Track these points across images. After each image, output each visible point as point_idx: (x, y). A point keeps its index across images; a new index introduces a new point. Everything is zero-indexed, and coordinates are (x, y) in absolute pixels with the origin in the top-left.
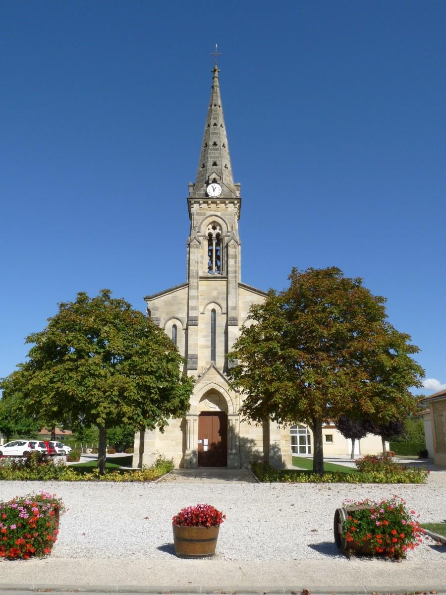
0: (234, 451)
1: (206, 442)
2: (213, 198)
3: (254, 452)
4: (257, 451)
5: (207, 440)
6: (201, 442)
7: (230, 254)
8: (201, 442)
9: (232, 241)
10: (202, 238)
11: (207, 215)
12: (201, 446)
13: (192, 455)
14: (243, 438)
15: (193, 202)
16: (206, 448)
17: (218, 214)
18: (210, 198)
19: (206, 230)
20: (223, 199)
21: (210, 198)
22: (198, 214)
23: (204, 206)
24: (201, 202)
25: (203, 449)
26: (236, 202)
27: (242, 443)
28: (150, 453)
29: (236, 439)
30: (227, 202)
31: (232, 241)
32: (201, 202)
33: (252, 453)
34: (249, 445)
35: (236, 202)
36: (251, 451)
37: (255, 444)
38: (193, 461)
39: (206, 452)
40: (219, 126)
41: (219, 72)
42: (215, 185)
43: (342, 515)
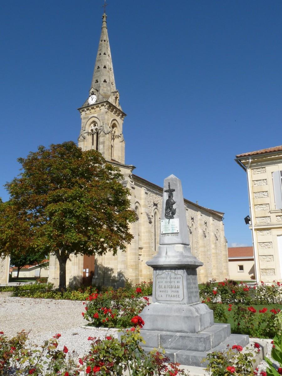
0: (96, 277)
1: (87, 270)
2: (91, 105)
3: (113, 277)
4: (114, 276)
5: (88, 269)
6: (84, 270)
7: (101, 141)
8: (84, 270)
9: (102, 132)
10: (86, 134)
11: (89, 118)
12: (85, 273)
13: (73, 279)
14: (106, 267)
15: (81, 111)
16: (87, 275)
17: (96, 115)
18: (90, 106)
19: (89, 128)
20: (97, 105)
21: (90, 106)
22: (85, 118)
23: (88, 112)
24: (85, 110)
25: (85, 276)
26: (105, 104)
27: (106, 271)
28: (52, 278)
29: (98, 269)
30: (100, 106)
31: (102, 132)
32: (85, 110)
33: (112, 278)
34: (110, 273)
35: (105, 104)
36: (111, 277)
37: (113, 272)
38: (73, 283)
39: (88, 277)
40: (107, 55)
41: (106, 17)
42: (94, 96)
43: (217, 325)
